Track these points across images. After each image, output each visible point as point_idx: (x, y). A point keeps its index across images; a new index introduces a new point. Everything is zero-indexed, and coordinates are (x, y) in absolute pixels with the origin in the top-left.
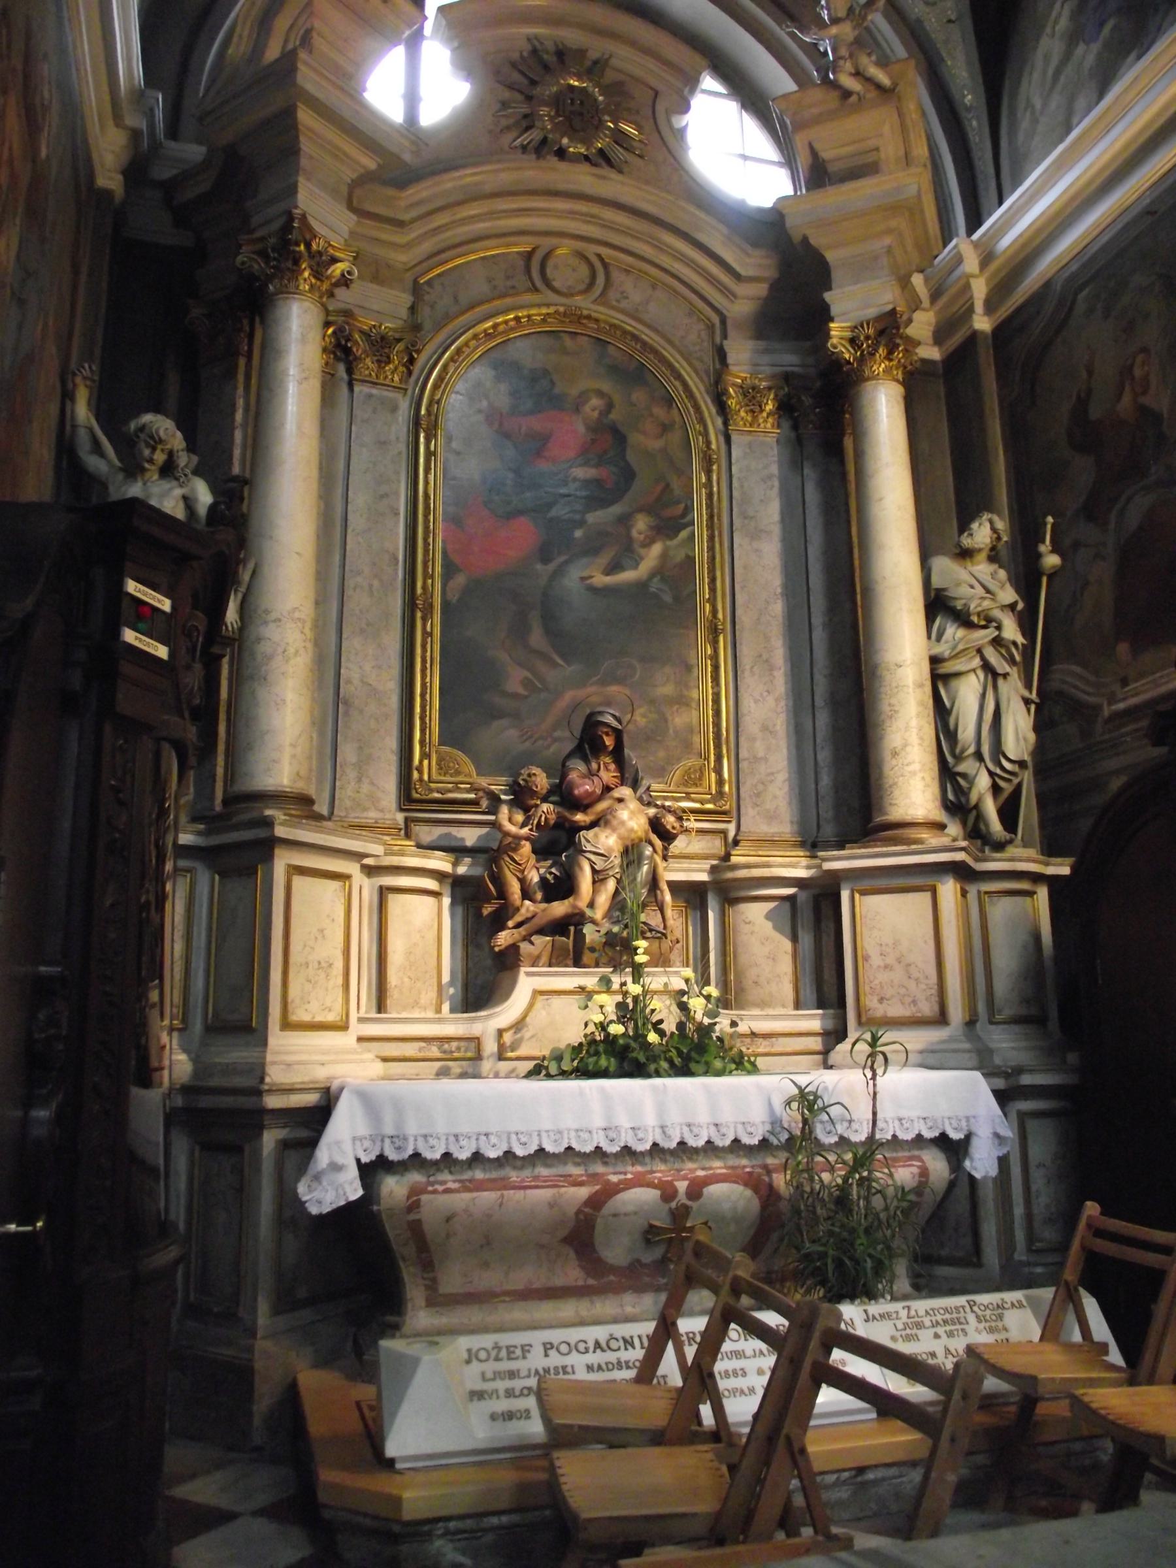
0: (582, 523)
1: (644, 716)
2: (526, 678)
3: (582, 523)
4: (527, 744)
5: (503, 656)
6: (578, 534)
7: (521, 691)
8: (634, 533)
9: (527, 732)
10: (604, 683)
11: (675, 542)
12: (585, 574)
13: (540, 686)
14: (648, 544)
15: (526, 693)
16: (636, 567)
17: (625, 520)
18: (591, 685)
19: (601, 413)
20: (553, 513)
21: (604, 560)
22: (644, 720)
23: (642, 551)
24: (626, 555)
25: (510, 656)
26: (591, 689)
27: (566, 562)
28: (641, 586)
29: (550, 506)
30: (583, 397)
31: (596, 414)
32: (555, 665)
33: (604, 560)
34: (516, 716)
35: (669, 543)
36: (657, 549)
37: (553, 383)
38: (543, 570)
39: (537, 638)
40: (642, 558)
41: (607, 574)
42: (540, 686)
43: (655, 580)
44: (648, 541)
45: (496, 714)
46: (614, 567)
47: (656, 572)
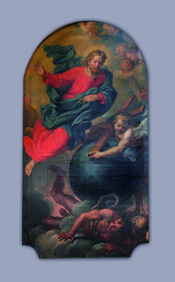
0: (88, 125)
1: (119, 223)
2: (61, 209)
3: (88, 125)
4: (63, 241)
5: (51, 200)
6: (87, 131)
7: (60, 216)
8: (116, 127)
9: (62, 235)
10: (100, 208)
11: (138, 128)
12: (90, 153)
13: (69, 213)
14: (122, 132)
15: (62, 217)
16: (117, 145)
17: (112, 120)
18: (95, 209)
19: (99, 63)
20: (75, 122)
21: (100, 144)
22: (119, 225)
23: (120, 136)
24: (114, 138)
25: (55, 199)
26: (93, 212)
27: (81, 148)
28: (119, 154)
29: (73, 120)
30: (90, 56)
31: (97, 64)
32: (76, 201)
33: (100, 144)
34: (57, 228)
35: (134, 129)
36: (127, 134)
37: (75, 53)
38: (70, 154)
39: (67, 189)
40: (120, 140)
41: (102, 151)
42: (69, 213)
43: (126, 151)
44: (123, 130)
45: (48, 227)
46: (106, 146)
47: (126, 146)
